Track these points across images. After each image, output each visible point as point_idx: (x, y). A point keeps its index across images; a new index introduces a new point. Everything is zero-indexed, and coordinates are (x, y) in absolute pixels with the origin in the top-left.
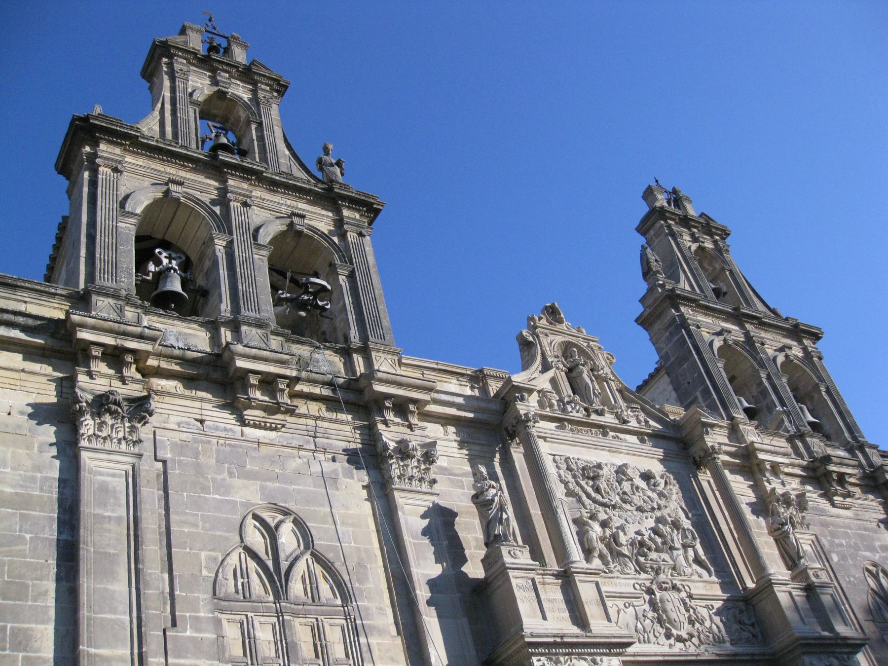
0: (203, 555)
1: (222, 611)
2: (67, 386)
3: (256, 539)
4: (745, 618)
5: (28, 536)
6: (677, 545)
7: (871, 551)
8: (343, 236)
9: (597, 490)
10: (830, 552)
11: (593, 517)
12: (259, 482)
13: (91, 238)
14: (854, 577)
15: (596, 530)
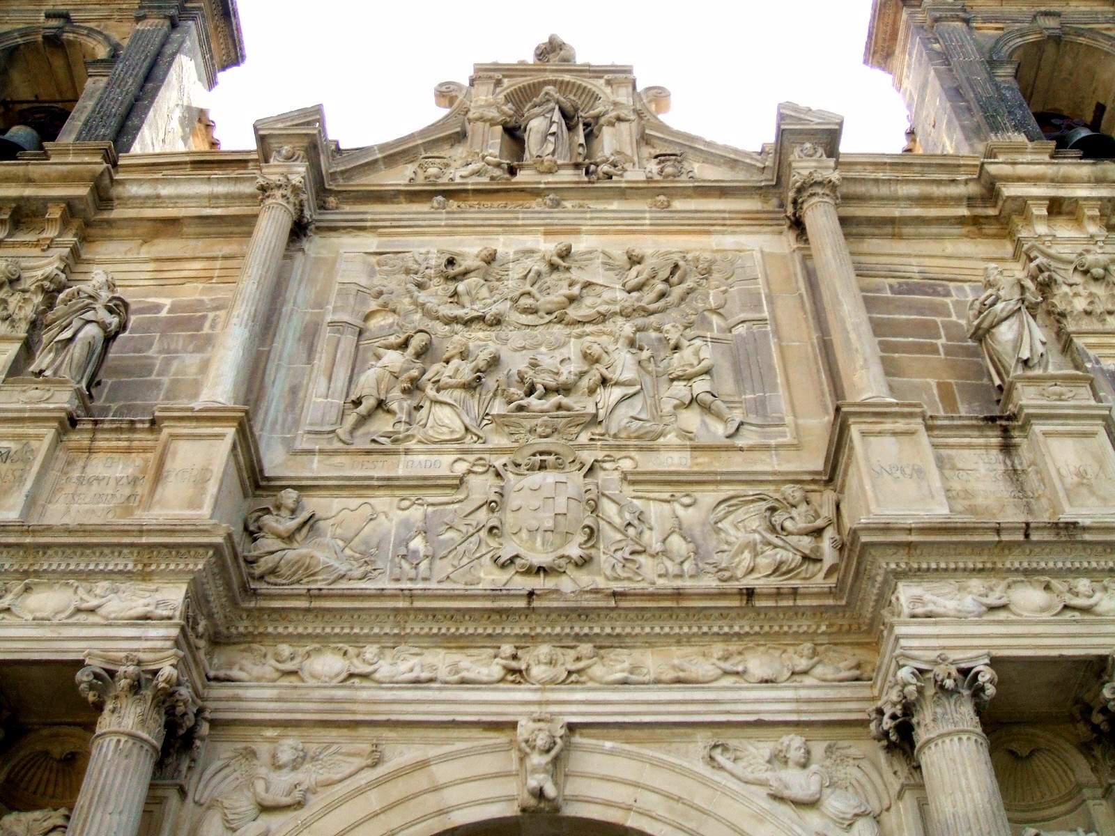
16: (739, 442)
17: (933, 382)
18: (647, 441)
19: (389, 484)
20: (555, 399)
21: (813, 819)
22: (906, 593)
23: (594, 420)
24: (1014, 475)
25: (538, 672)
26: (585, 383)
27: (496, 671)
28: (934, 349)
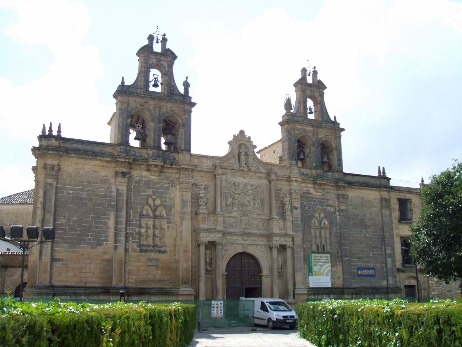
0: (139, 206)
1: (141, 218)
5: (107, 203)
7: (321, 206)
9: (235, 190)
10: (305, 206)
12: (152, 190)
14: (310, 214)
16: (261, 214)
17: (278, 205)
18: (253, 213)
20: (246, 208)
21: (263, 253)
22: (274, 238)
23: (249, 211)
24: (284, 225)
25: (245, 239)
26: (249, 205)
27: (241, 239)
28: (278, 200)
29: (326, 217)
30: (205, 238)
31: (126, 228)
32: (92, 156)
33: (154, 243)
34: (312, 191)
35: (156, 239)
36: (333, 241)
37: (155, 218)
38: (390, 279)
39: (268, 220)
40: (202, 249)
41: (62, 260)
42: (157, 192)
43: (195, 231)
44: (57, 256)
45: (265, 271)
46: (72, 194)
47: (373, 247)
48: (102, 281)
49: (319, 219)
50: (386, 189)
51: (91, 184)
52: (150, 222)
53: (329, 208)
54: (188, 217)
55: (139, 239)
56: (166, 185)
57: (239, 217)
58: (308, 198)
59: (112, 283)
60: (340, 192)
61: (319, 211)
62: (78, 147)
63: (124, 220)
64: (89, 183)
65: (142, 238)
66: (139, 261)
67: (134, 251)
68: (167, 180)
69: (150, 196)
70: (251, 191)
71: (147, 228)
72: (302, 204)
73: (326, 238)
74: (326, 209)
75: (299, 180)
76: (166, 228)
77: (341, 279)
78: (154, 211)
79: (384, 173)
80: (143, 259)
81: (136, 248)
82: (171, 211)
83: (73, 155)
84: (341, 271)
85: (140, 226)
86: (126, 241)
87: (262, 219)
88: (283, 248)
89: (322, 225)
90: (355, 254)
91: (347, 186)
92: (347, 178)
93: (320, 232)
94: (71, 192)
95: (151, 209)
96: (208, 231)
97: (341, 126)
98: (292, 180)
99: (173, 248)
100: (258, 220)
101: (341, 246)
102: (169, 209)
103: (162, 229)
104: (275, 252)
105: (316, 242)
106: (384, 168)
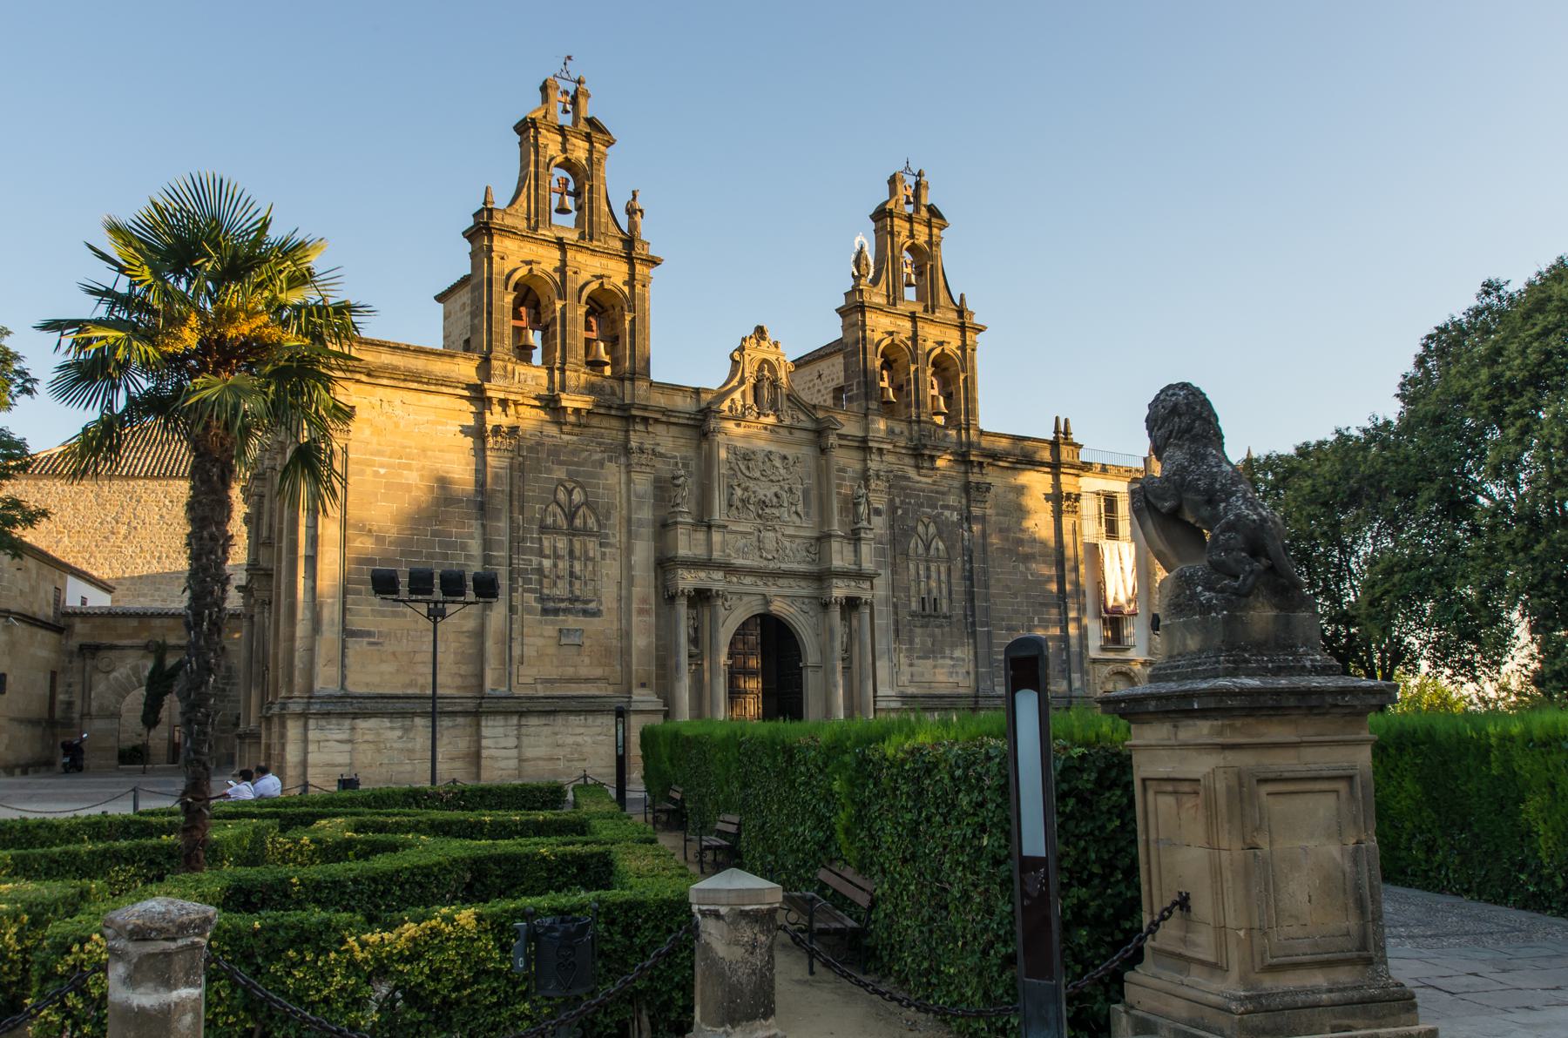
2: (480, 416)
3: (562, 496)
4: (811, 549)
6: (785, 504)
8: (632, 287)
9: (748, 468)
10: (897, 508)
11: (739, 485)
13: (490, 313)
15: (739, 492)
18: (786, 524)
19: (741, 533)
29: (940, 534)
30: (688, 580)
31: (511, 558)
32: (427, 383)
33: (572, 592)
34: (912, 473)
35: (577, 584)
36: (955, 588)
37: (574, 535)
38: (1075, 676)
39: (818, 539)
40: (682, 607)
41: (369, 634)
42: (578, 473)
43: (665, 564)
44: (356, 623)
45: (811, 656)
46: (384, 476)
47: (1041, 604)
48: (458, 681)
49: (924, 538)
50: (1072, 471)
51: (429, 453)
52: (562, 544)
53: (947, 513)
54: (647, 532)
55: (541, 583)
56: (597, 457)
57: (756, 533)
58: (903, 488)
59: (481, 685)
60: (974, 478)
61: (926, 520)
62: (395, 363)
63: (505, 539)
64: (424, 450)
65: (545, 580)
66: (541, 636)
67: (530, 611)
68: (600, 444)
69: (561, 483)
70: (782, 471)
71: (556, 556)
72: (891, 501)
73: (939, 581)
74: (942, 514)
75: (885, 446)
76: (598, 558)
77: (972, 676)
78: (571, 517)
79: (1066, 433)
80: (550, 631)
81: (534, 604)
82: (608, 518)
83: (385, 382)
84: (971, 657)
85: (541, 554)
86: (512, 590)
87: (805, 538)
88: (851, 604)
89: (932, 551)
90: (1003, 620)
91: (989, 464)
92: (985, 442)
93: (928, 569)
94: (382, 471)
95: (562, 509)
96: (694, 564)
97: (977, 320)
98: (871, 448)
99: (615, 605)
100: (797, 541)
101: (972, 600)
102: (602, 515)
103: (588, 559)
104: (836, 613)
105: (919, 592)
106: (1066, 421)
